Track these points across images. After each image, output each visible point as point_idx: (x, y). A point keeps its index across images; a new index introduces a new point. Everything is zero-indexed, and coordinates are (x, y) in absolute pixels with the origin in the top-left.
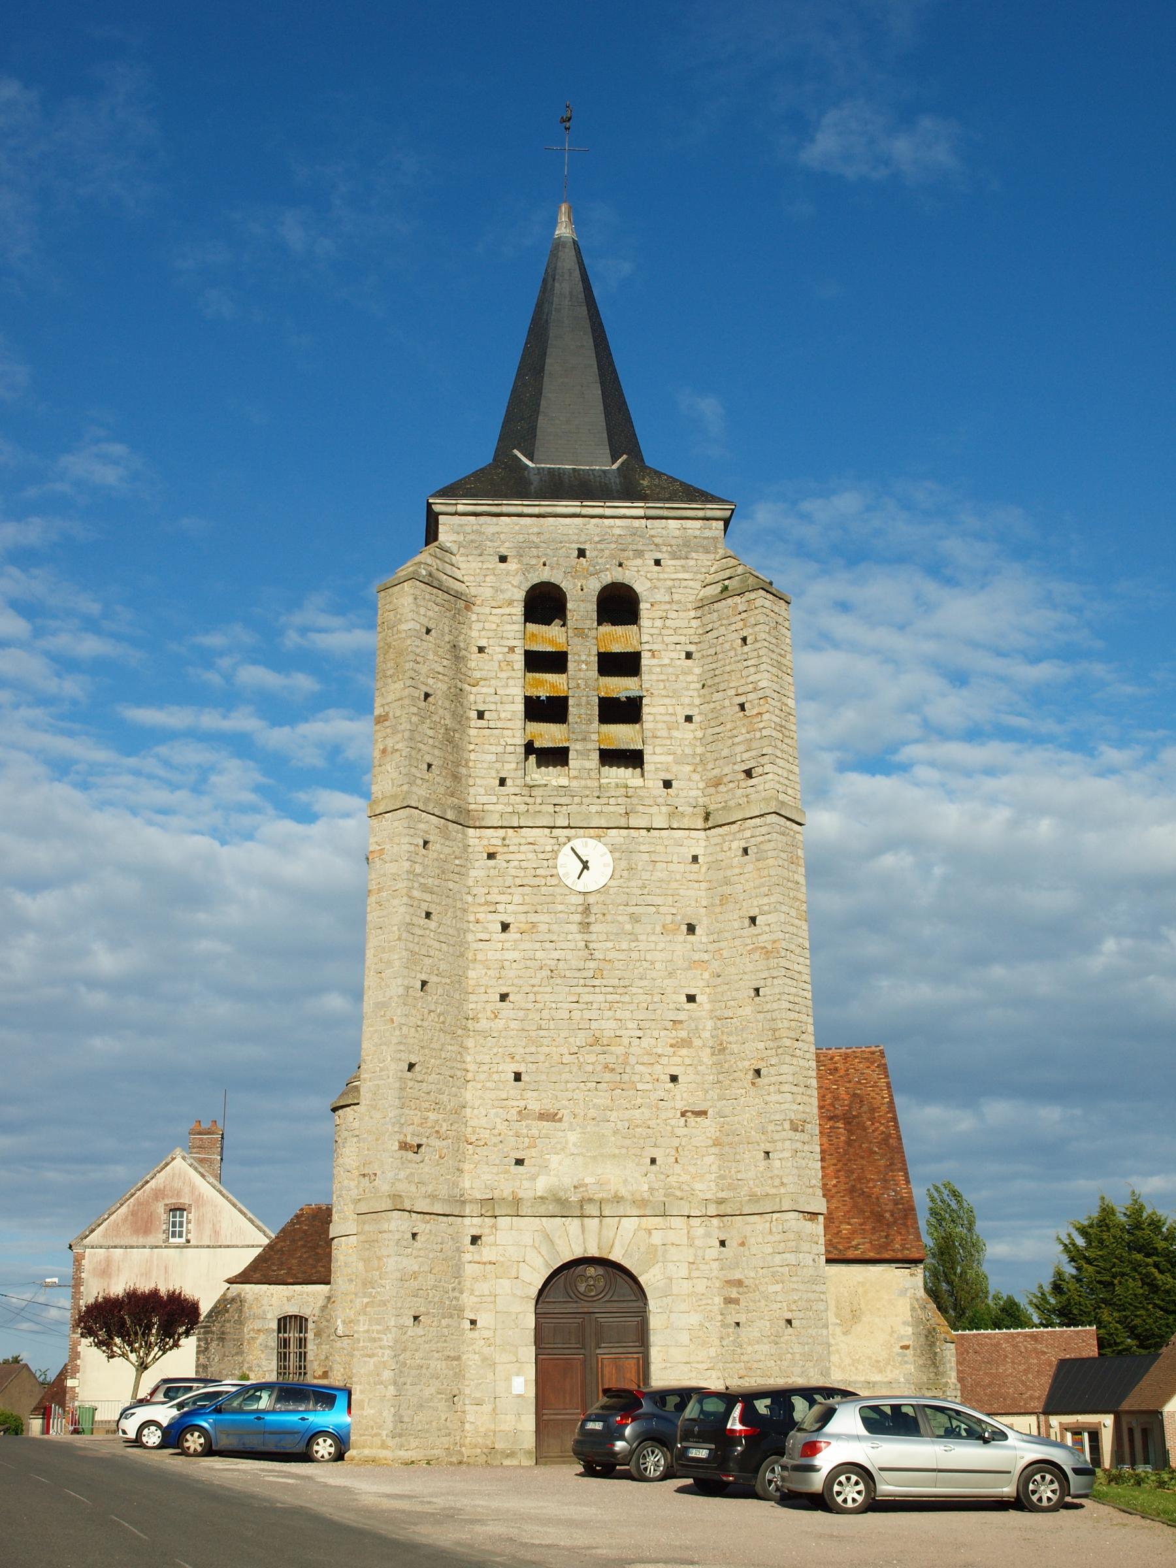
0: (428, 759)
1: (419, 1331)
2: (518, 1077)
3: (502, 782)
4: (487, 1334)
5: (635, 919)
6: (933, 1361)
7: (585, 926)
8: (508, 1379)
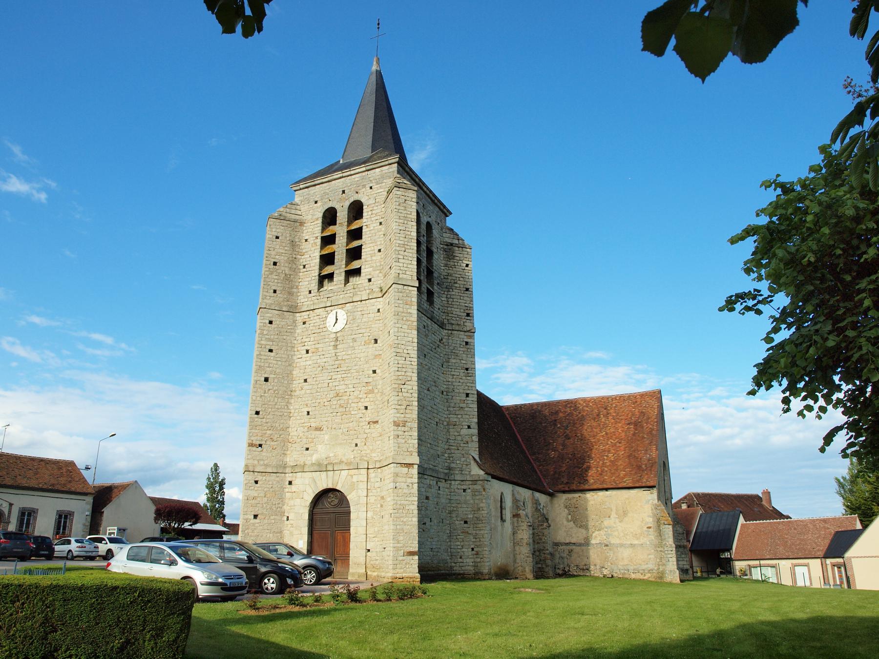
0: (274, 288)
1: (257, 521)
2: (308, 413)
3: (310, 292)
4: (292, 522)
5: (354, 340)
6: (660, 534)
7: (336, 346)
8: (297, 541)
